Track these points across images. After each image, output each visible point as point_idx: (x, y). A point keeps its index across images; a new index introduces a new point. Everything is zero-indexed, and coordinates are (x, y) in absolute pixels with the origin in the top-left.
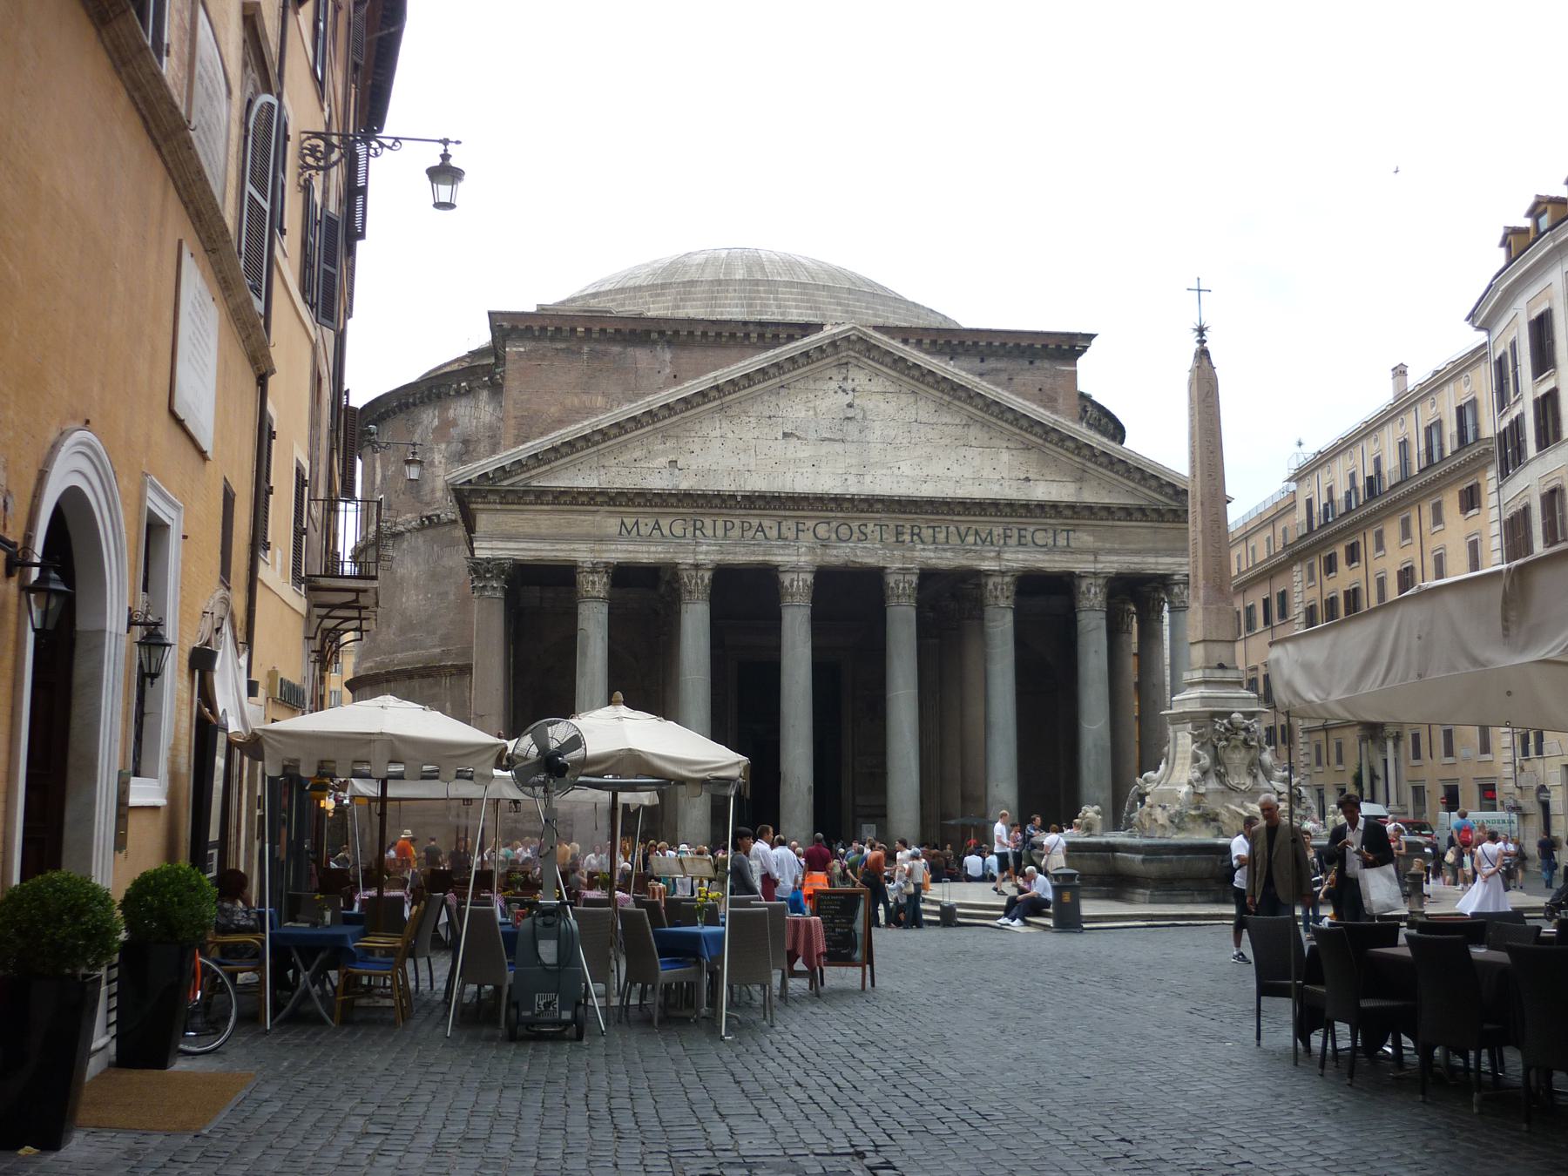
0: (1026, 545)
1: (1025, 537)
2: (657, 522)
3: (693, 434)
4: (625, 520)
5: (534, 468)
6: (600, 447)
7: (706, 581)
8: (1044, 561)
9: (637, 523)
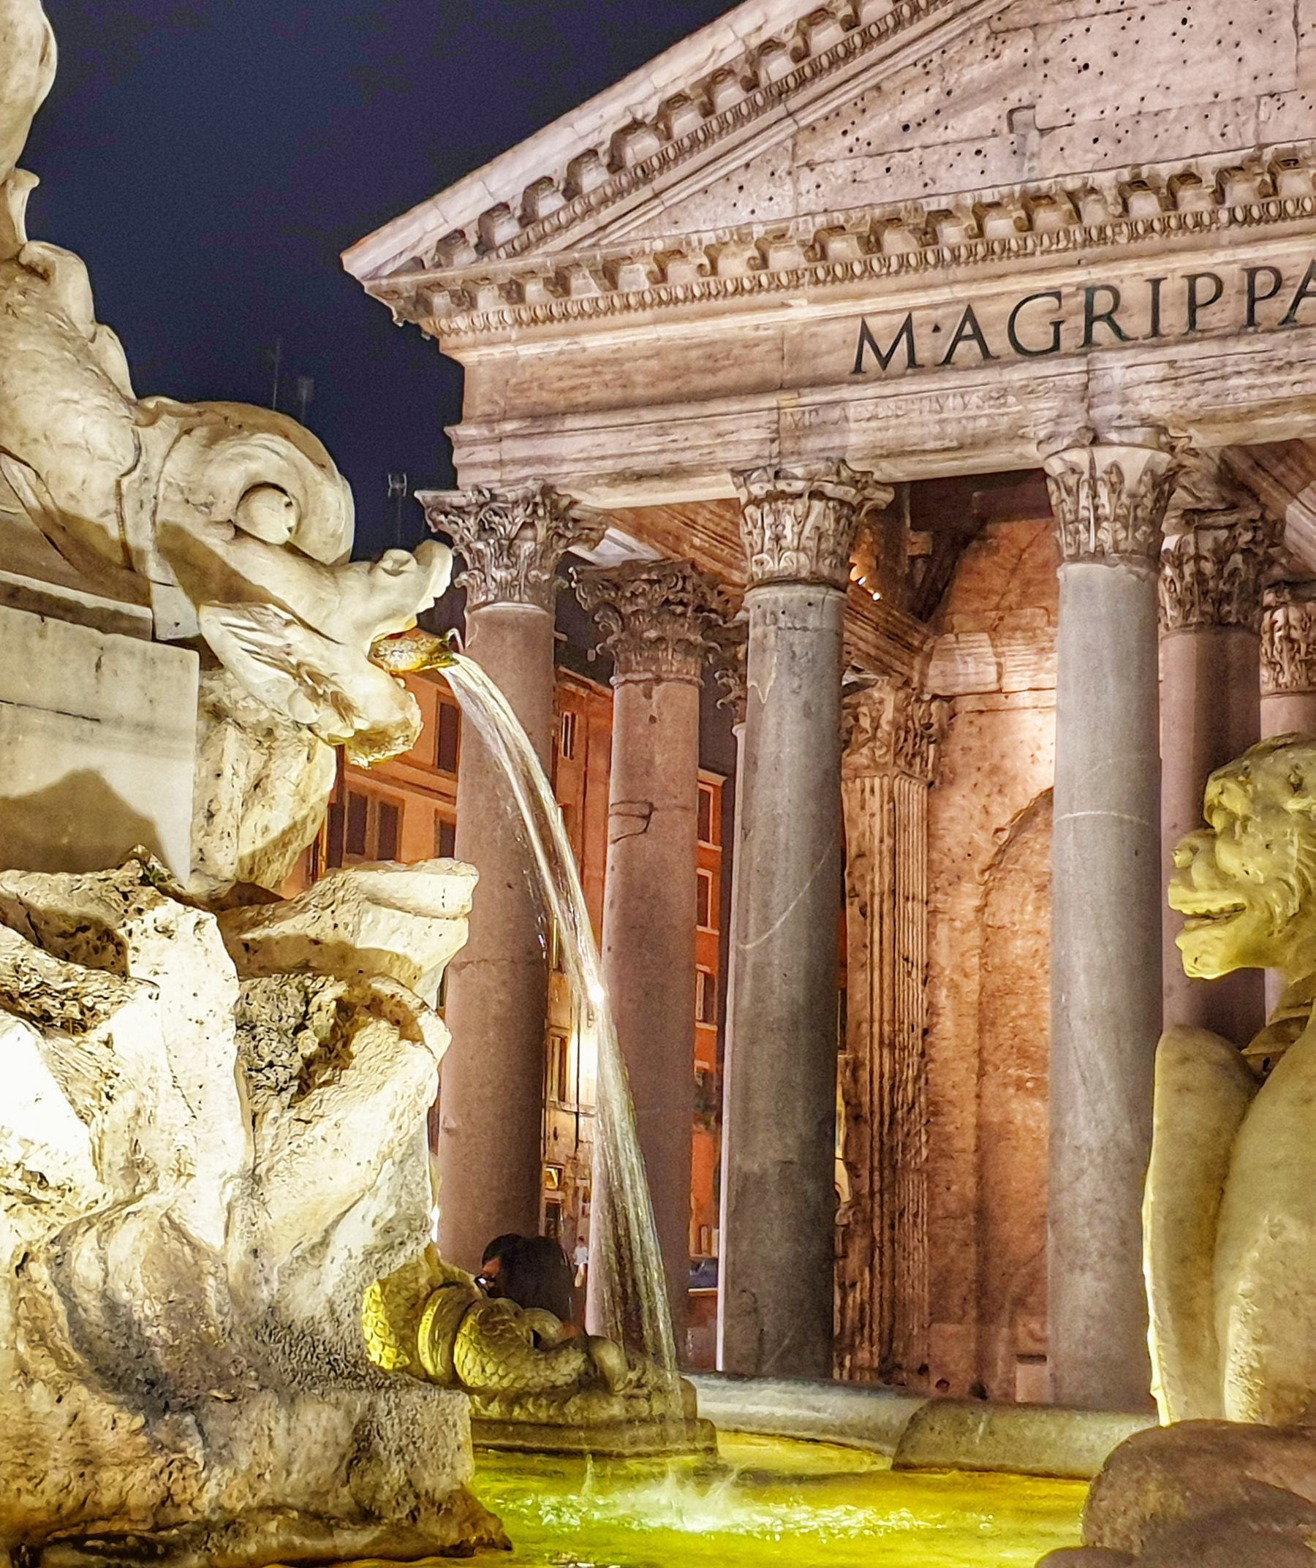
2: (969, 316)
4: (871, 322)
5: (605, 202)
6: (794, 102)
9: (908, 327)
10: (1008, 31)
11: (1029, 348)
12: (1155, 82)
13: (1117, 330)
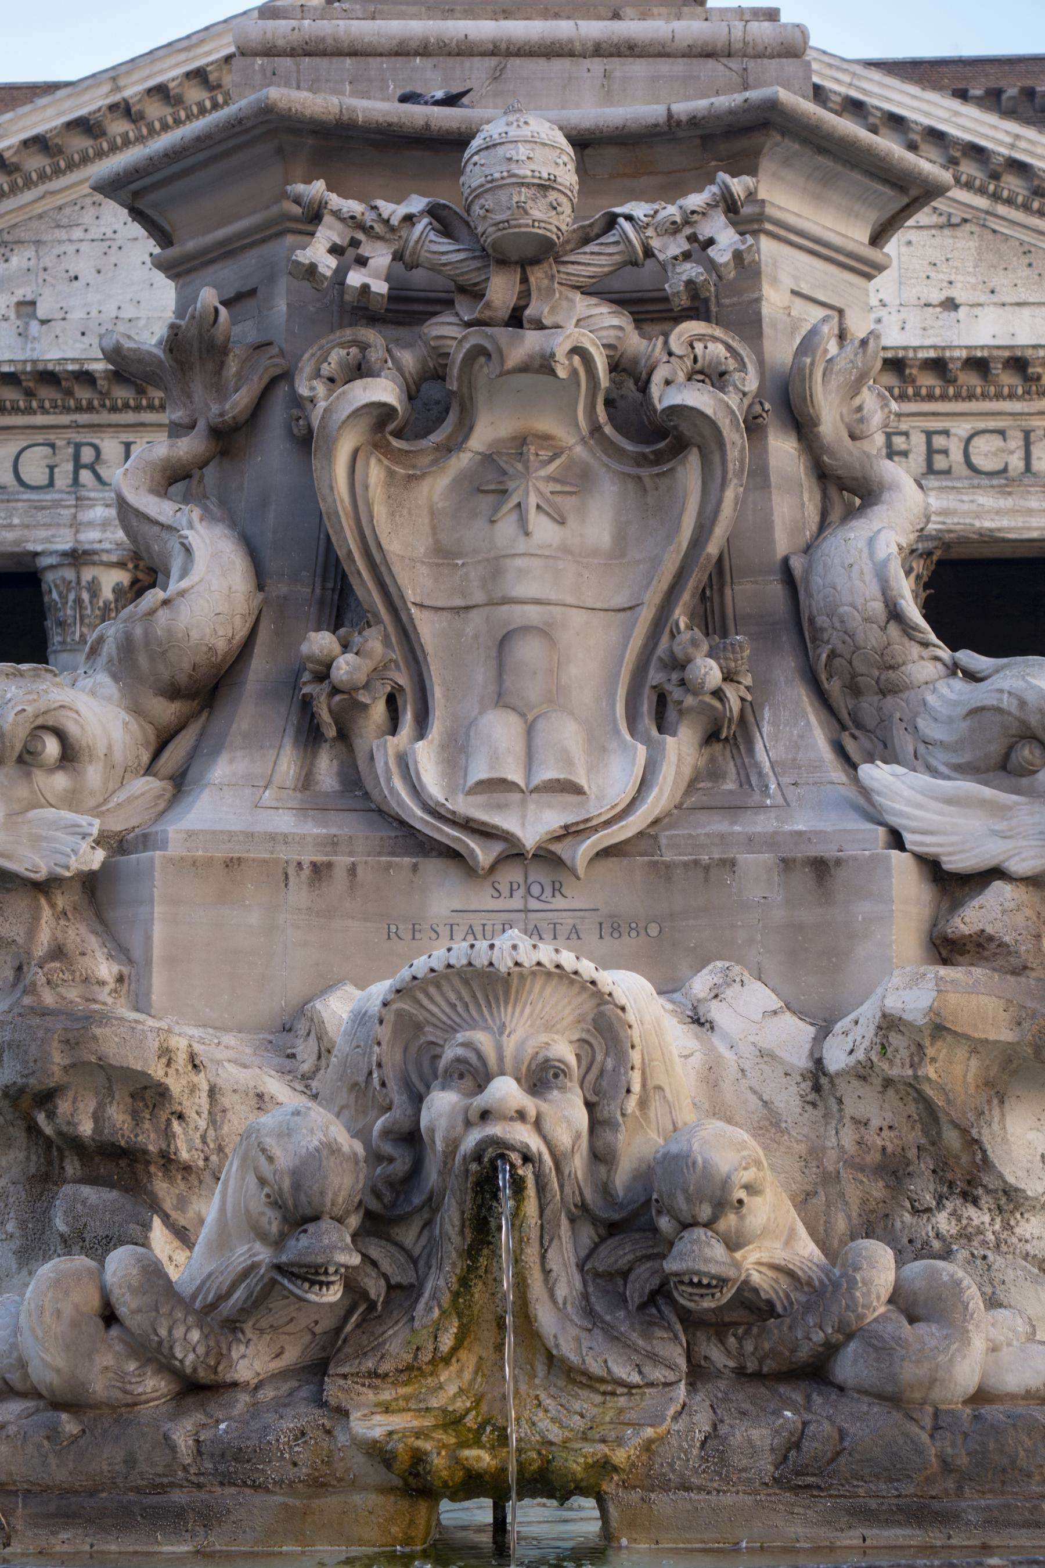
0: (947, 472)
1: (945, 452)
3: (77, 233)
7: (107, 594)
8: (998, 512)
10: (16, 242)
11: (33, 483)
12: (129, 297)
13: (98, 477)
